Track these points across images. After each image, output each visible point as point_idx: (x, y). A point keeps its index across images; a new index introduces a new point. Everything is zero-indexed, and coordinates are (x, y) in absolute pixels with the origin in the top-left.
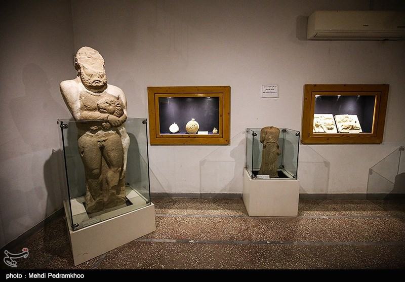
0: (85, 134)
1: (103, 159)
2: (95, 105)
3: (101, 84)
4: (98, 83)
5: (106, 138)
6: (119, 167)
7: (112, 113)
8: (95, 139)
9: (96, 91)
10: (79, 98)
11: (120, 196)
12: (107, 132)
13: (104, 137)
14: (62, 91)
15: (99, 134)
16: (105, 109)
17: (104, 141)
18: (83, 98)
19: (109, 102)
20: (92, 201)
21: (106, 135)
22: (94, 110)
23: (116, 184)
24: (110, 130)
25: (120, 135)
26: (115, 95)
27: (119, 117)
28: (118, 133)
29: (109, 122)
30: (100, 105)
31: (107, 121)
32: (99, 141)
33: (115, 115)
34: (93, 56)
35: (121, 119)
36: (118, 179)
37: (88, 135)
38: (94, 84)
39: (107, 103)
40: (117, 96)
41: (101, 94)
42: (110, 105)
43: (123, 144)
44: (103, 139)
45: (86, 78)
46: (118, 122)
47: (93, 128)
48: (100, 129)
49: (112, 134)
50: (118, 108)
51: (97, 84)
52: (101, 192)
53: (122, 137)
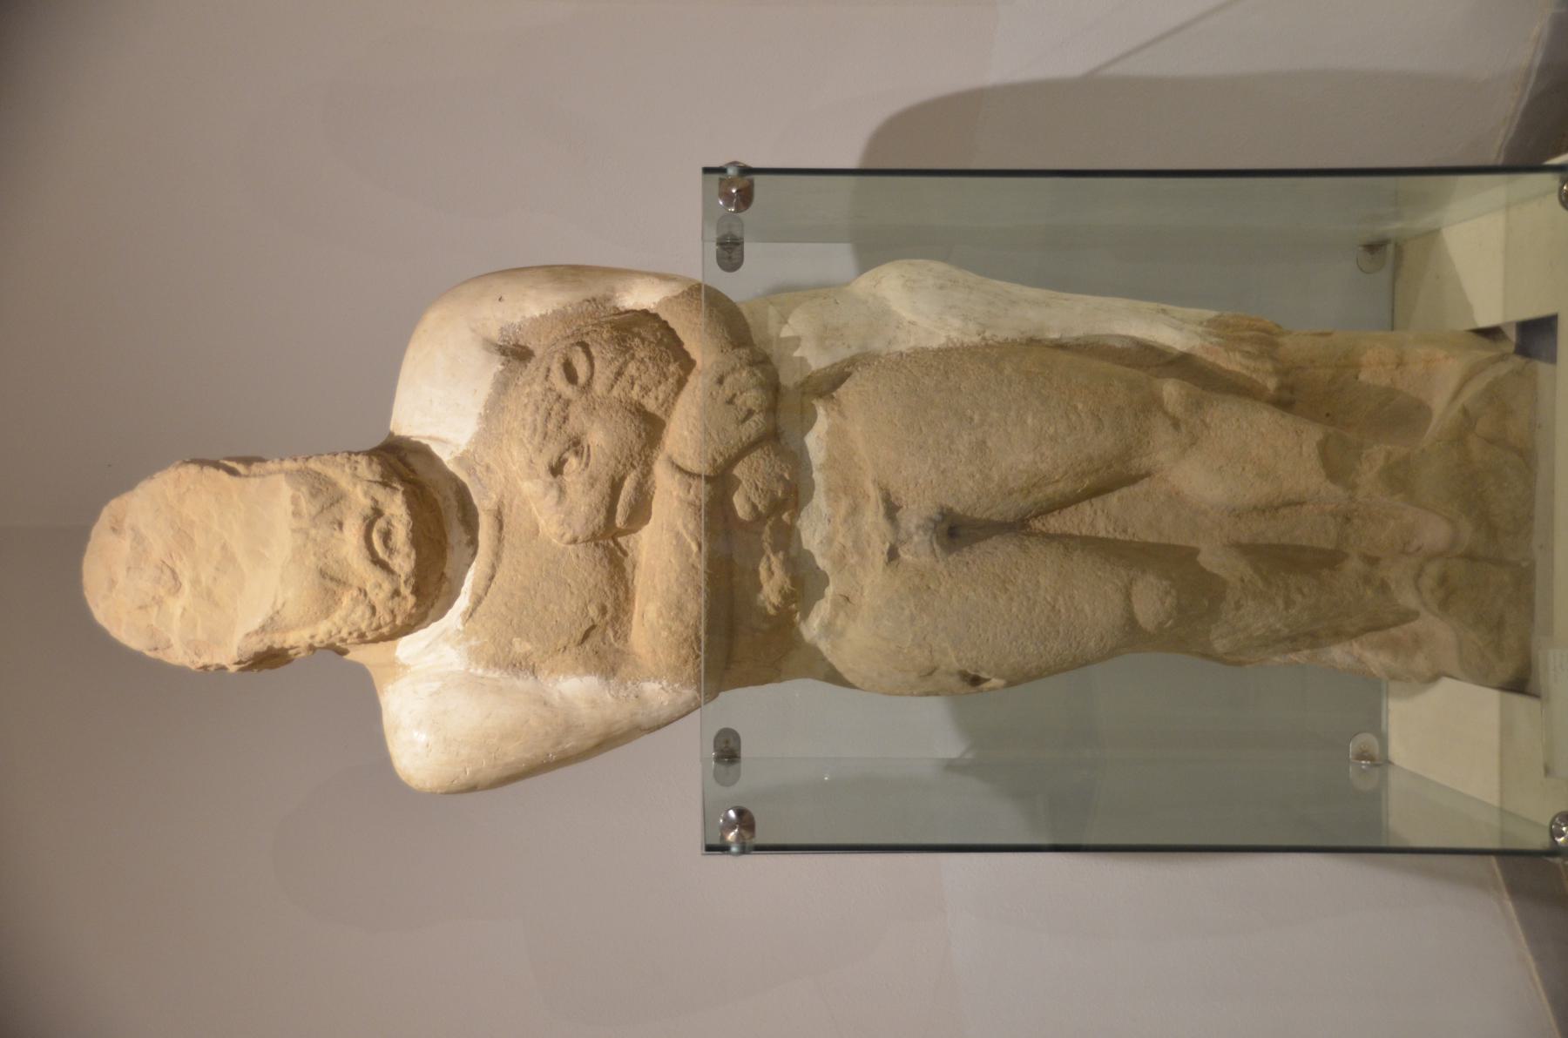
0: (824, 646)
1: (1054, 523)
2: (584, 569)
3: (396, 508)
4: (386, 536)
5: (874, 493)
6: (1152, 404)
7: (651, 427)
8: (872, 580)
9: (456, 535)
10: (524, 684)
11: (1441, 404)
12: (818, 477)
13: (855, 510)
14: (472, 788)
15: (829, 540)
16: (616, 487)
17: (891, 510)
18: (520, 647)
19: (552, 451)
20: (1417, 642)
21: (846, 488)
22: (617, 565)
23: (1314, 434)
24: (798, 460)
25: (852, 362)
26: (485, 388)
27: (687, 364)
28: (829, 384)
29: (732, 462)
30: (579, 527)
31: (720, 482)
32: (893, 555)
33: (669, 403)
34: (158, 550)
35: (695, 344)
36: (1266, 418)
37: (828, 628)
38: (403, 563)
39: (556, 470)
40: (497, 365)
41: (484, 504)
42: (576, 445)
43: (938, 341)
44: (873, 515)
45: (347, 616)
46: (727, 390)
47: (771, 587)
48: (786, 538)
49: (836, 434)
50: (603, 374)
51: (401, 534)
52: (1354, 565)
53: (878, 345)
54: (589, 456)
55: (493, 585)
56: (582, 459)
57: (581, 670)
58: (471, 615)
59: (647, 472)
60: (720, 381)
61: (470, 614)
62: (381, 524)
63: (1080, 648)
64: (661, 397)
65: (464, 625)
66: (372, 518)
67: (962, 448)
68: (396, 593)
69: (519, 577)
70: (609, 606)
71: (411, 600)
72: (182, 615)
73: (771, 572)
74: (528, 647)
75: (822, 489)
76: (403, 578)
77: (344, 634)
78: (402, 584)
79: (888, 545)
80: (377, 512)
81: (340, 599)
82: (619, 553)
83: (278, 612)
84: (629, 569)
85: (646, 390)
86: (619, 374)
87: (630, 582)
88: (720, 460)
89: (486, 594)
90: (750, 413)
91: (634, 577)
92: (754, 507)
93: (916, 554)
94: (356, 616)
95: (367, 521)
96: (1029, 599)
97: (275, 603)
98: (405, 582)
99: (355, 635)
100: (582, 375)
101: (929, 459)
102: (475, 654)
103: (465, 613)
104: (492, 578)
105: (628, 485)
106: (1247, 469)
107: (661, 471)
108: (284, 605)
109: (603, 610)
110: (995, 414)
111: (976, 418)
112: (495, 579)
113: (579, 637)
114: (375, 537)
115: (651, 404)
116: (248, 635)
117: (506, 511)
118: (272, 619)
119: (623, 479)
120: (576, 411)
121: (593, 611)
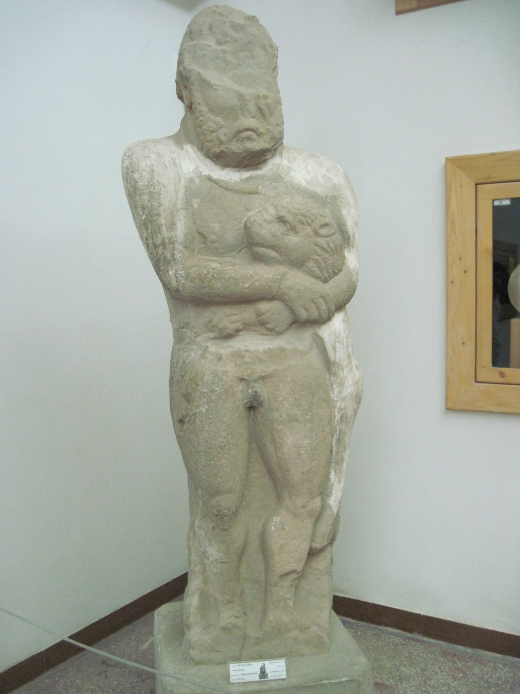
4: (249, 138)
17: (263, 378)
18: (196, 202)
33: (310, 273)
38: (235, 147)
44: (260, 369)
54: (288, 235)
55: (223, 190)
56: (286, 232)
57: (186, 231)
58: (209, 179)
59: (280, 263)
60: (322, 297)
61: (209, 179)
62: (254, 136)
63: (202, 472)
64: (312, 269)
65: (204, 176)
66: (257, 132)
67: (294, 411)
68: (221, 143)
69: (228, 202)
70: (215, 245)
71: (218, 150)
72: (208, 45)
73: (233, 322)
74: (196, 206)
75: (271, 347)
76: (228, 146)
77: (201, 118)
78: (225, 146)
79: (247, 378)
80: (259, 135)
81: (219, 116)
82: (239, 249)
83: (212, 87)
84: (232, 254)
85: (316, 262)
86: (323, 248)
87: (226, 255)
88: (286, 297)
89: (219, 186)
90: (307, 310)
91: (228, 257)
92: (263, 314)
93: (242, 391)
94: (210, 123)
95: (256, 130)
96: (225, 446)
97: (216, 85)
98: (227, 147)
99: (200, 123)
100: (323, 232)
101: (288, 396)
102: (191, 180)
103: (210, 176)
104: (227, 189)
105: (273, 254)
106: (284, 540)
107: (282, 269)
108: (216, 90)
109: (213, 242)
110: (309, 425)
111: (307, 417)
112: (226, 191)
113: (201, 231)
114: (249, 133)
115: (310, 264)
116: (199, 74)
117: (257, 196)
118: (209, 84)
119: (276, 251)
120: (309, 230)
121: (213, 237)
